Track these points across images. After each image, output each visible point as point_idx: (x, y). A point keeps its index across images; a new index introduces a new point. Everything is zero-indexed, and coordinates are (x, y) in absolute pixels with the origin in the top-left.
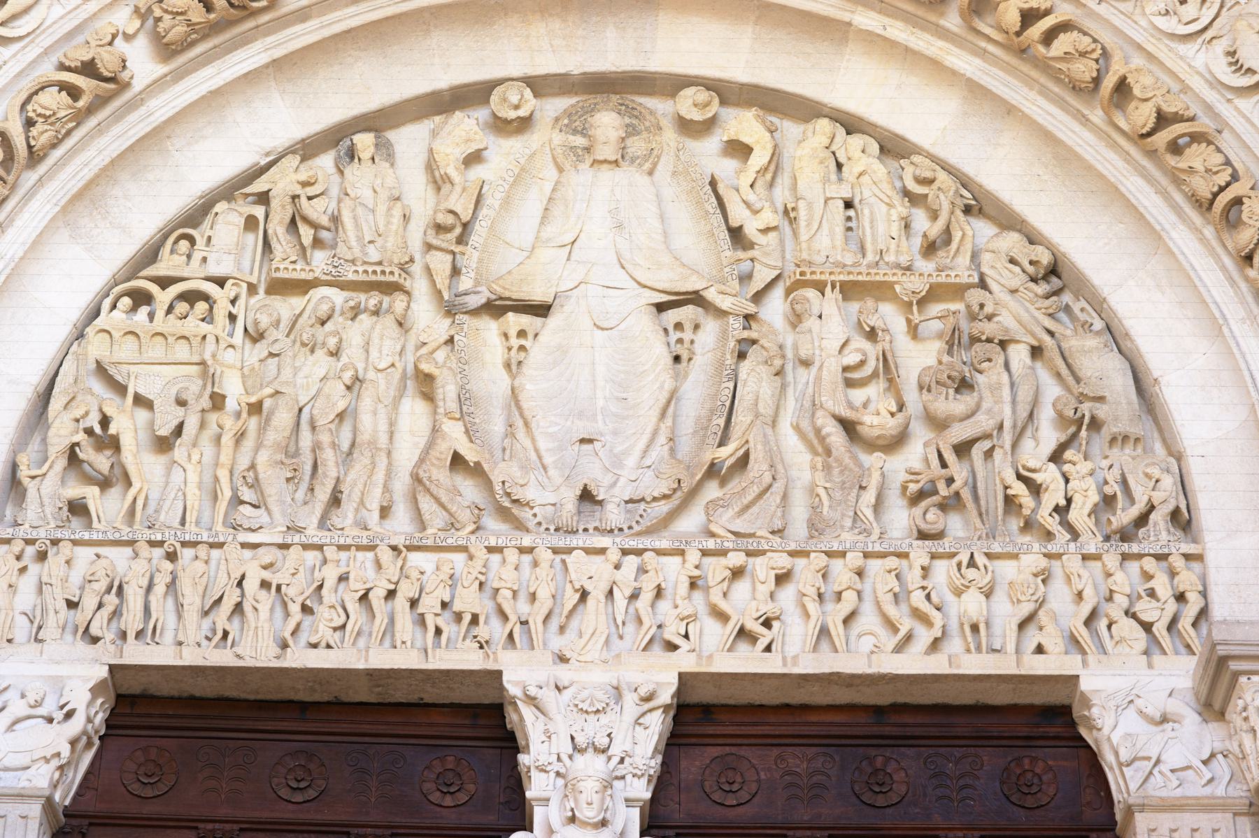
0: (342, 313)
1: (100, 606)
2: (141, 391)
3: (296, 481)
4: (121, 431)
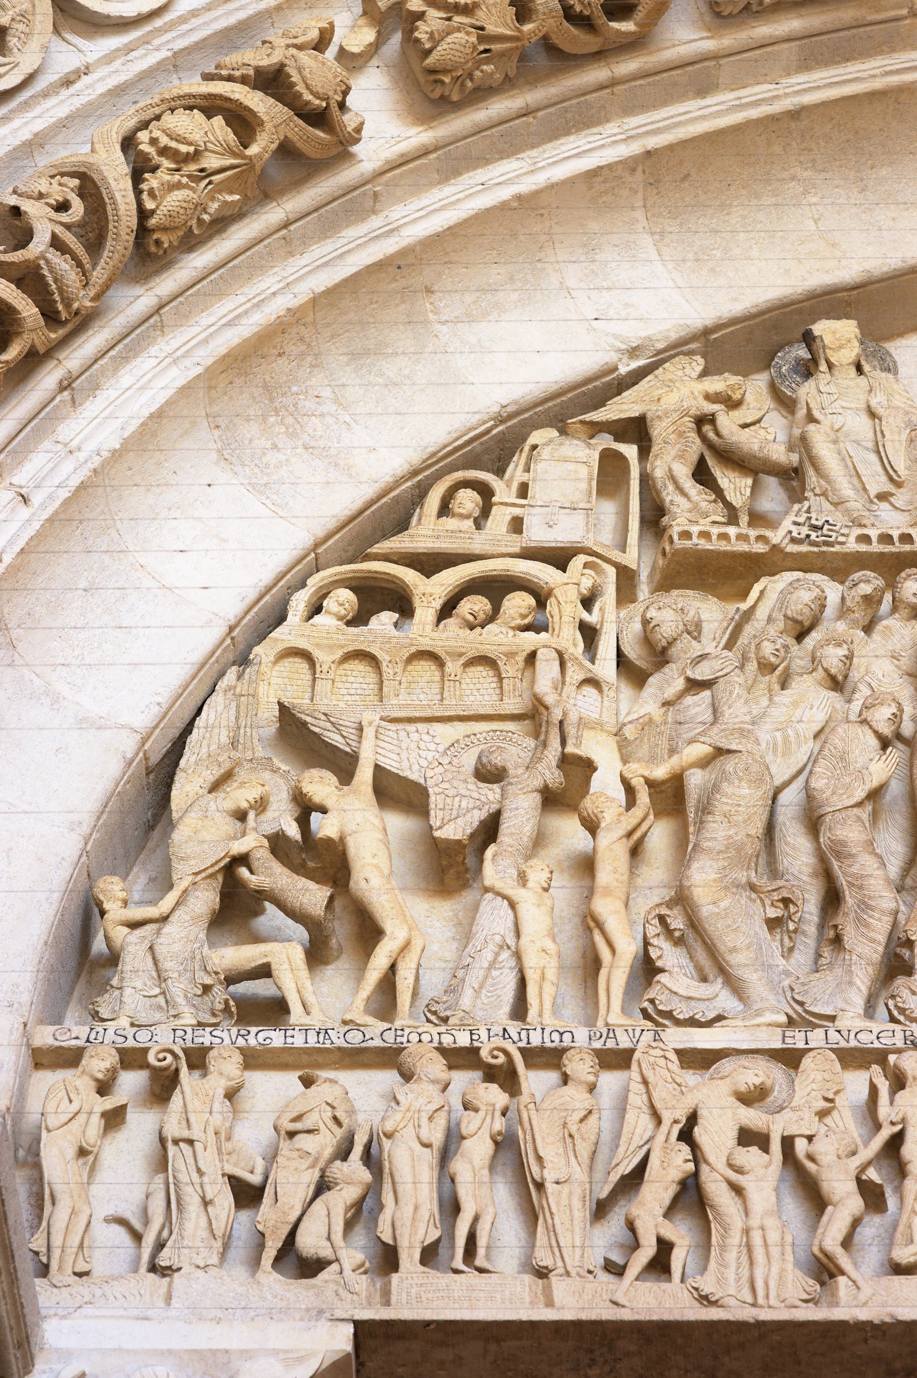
0: (843, 611)
1: (322, 1187)
2: (391, 763)
3: (792, 926)
4: (350, 827)
